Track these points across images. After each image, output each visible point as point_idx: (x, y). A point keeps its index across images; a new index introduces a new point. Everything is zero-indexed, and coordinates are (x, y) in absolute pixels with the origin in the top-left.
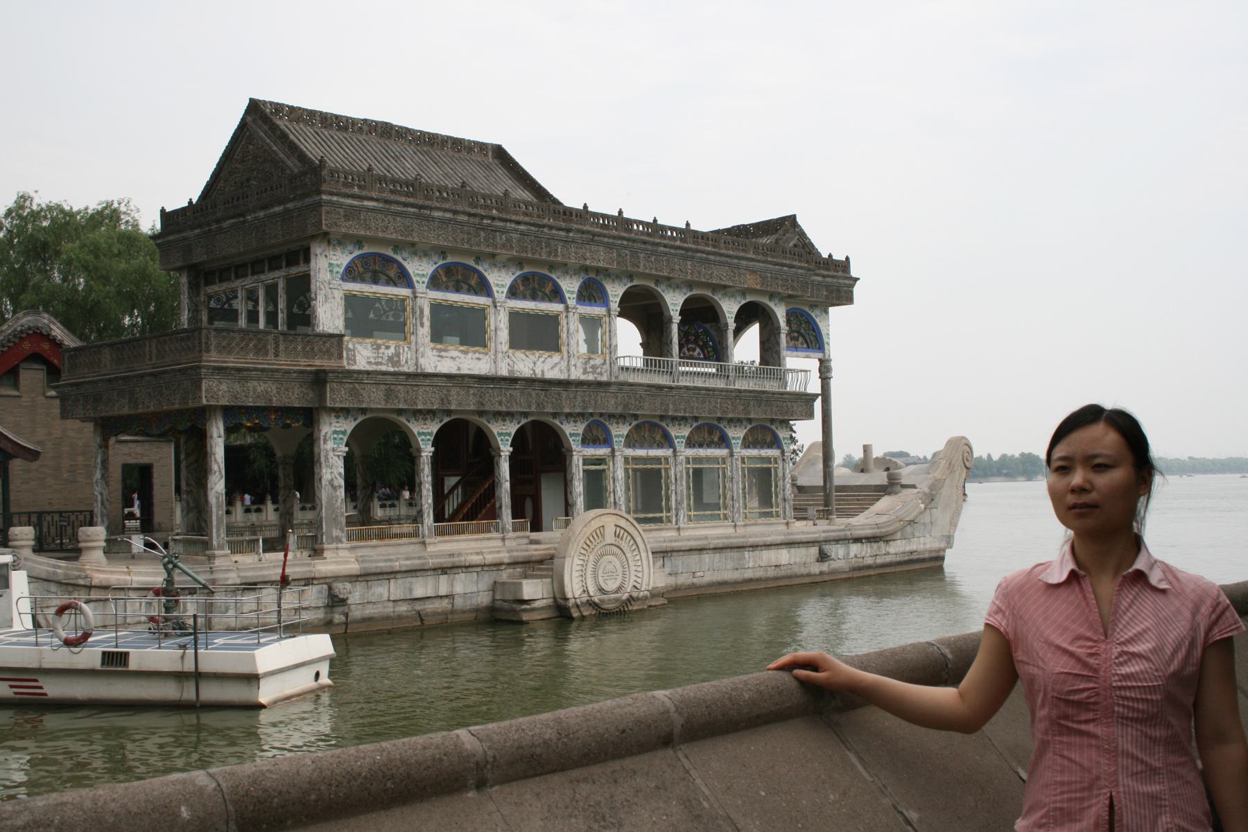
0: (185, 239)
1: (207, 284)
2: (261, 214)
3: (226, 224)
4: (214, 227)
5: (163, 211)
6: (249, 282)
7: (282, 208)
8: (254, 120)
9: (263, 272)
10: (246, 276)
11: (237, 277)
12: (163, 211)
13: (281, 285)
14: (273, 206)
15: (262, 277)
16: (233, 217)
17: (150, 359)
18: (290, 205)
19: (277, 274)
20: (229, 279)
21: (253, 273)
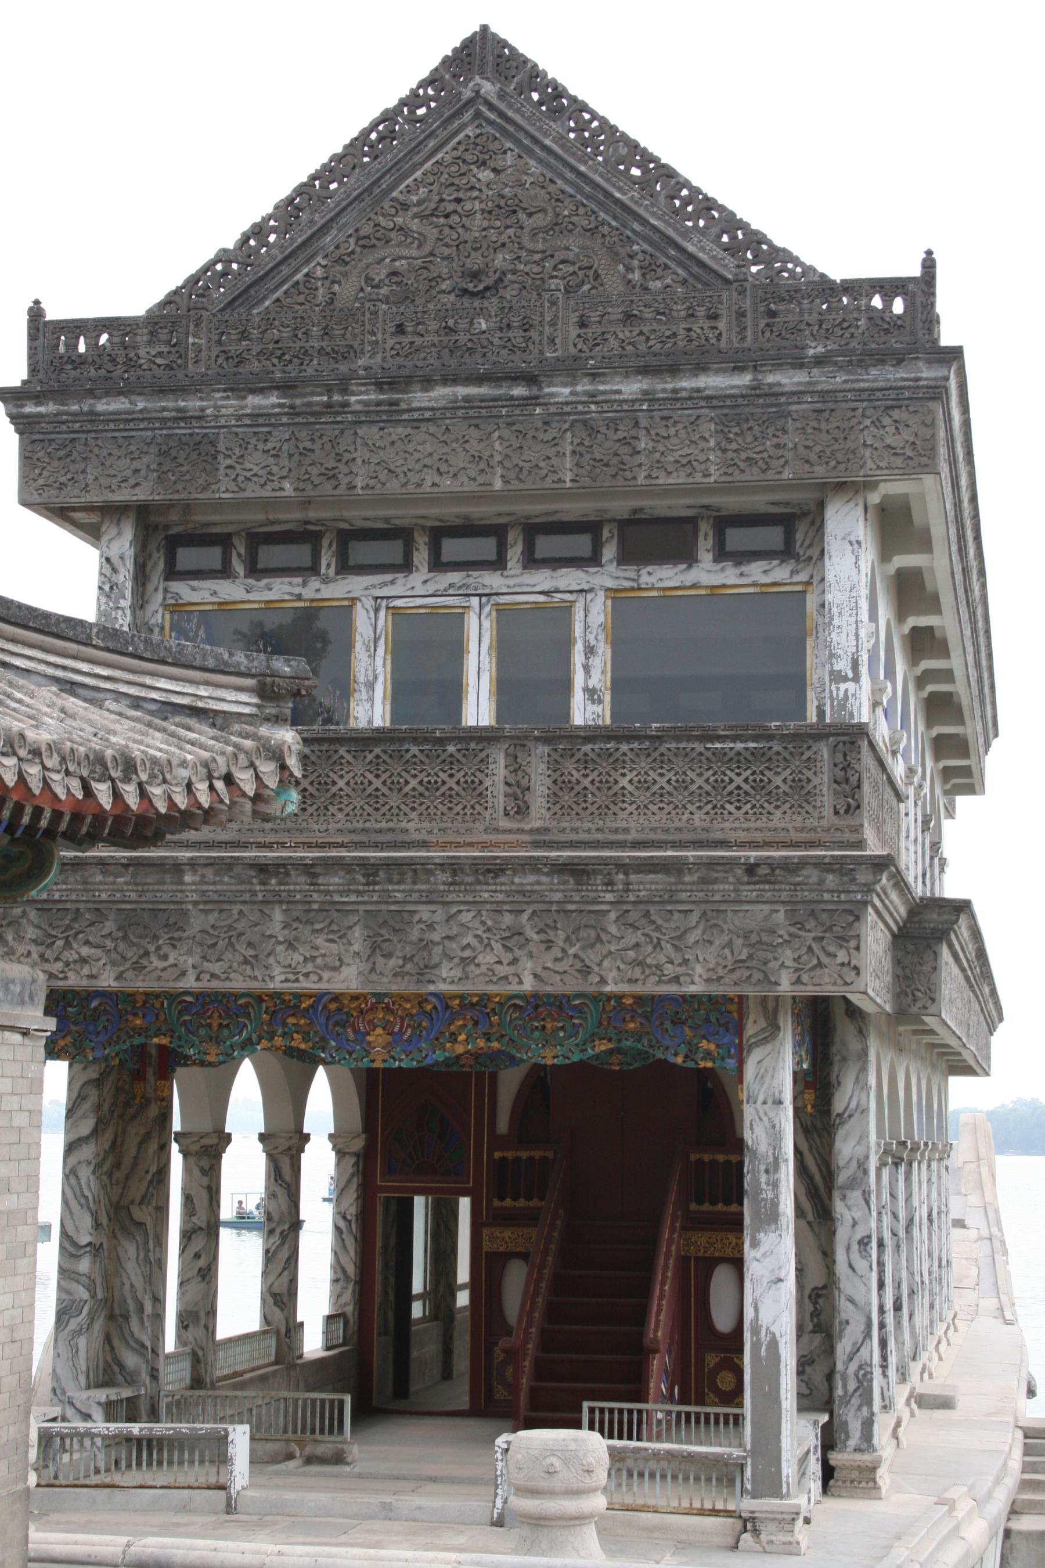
0: (183, 417)
1: (172, 573)
2: (631, 388)
3: (420, 398)
4: (361, 397)
5: (36, 313)
6: (418, 588)
7: (745, 379)
8: (502, 95)
9: (499, 564)
10: (406, 566)
11: (345, 567)
12: (36, 313)
13: (591, 620)
14: (701, 368)
15: (492, 580)
16: (480, 380)
17: (522, 810)
18: (788, 379)
19: (569, 578)
20: (314, 569)
21: (437, 565)
